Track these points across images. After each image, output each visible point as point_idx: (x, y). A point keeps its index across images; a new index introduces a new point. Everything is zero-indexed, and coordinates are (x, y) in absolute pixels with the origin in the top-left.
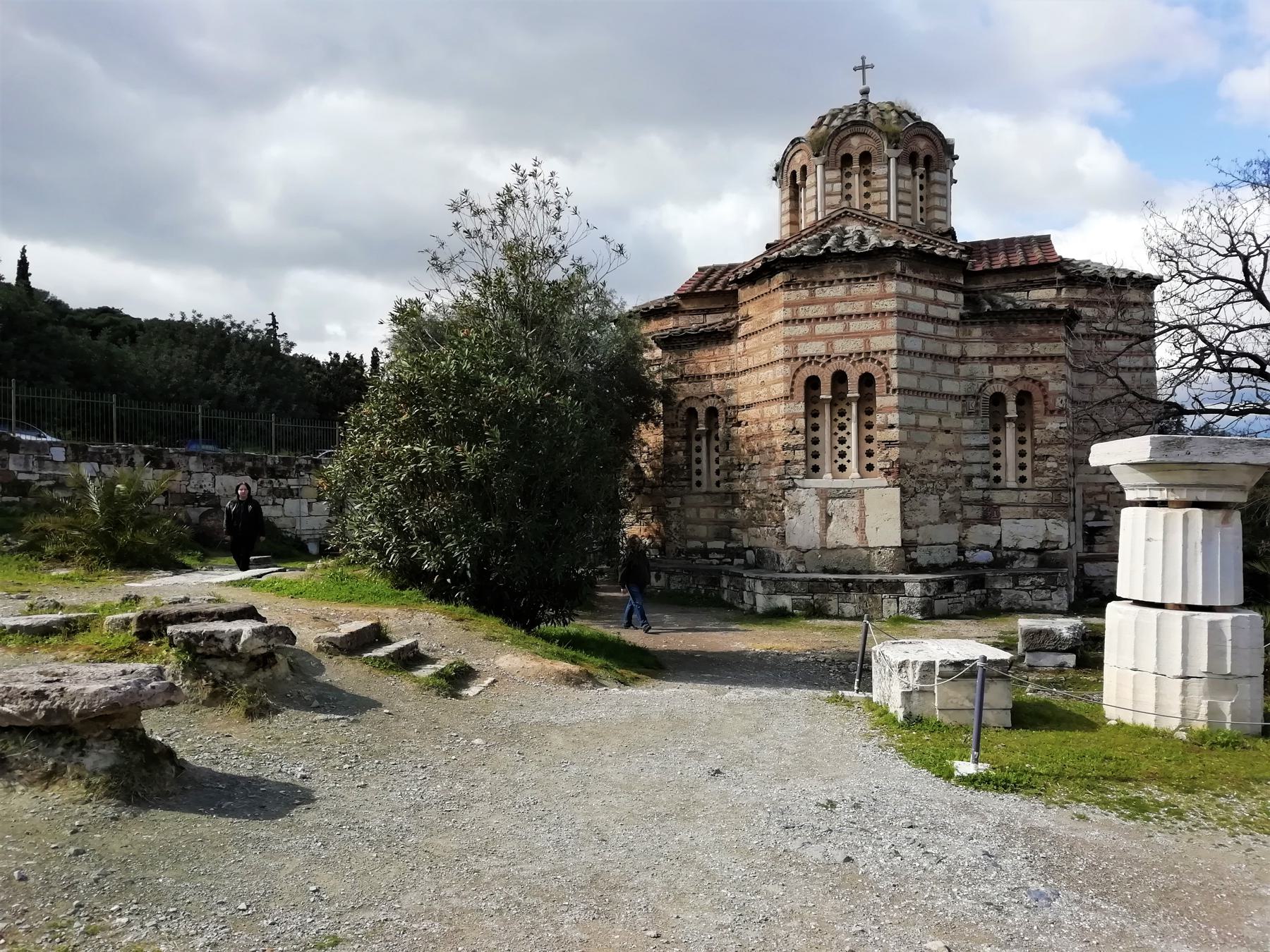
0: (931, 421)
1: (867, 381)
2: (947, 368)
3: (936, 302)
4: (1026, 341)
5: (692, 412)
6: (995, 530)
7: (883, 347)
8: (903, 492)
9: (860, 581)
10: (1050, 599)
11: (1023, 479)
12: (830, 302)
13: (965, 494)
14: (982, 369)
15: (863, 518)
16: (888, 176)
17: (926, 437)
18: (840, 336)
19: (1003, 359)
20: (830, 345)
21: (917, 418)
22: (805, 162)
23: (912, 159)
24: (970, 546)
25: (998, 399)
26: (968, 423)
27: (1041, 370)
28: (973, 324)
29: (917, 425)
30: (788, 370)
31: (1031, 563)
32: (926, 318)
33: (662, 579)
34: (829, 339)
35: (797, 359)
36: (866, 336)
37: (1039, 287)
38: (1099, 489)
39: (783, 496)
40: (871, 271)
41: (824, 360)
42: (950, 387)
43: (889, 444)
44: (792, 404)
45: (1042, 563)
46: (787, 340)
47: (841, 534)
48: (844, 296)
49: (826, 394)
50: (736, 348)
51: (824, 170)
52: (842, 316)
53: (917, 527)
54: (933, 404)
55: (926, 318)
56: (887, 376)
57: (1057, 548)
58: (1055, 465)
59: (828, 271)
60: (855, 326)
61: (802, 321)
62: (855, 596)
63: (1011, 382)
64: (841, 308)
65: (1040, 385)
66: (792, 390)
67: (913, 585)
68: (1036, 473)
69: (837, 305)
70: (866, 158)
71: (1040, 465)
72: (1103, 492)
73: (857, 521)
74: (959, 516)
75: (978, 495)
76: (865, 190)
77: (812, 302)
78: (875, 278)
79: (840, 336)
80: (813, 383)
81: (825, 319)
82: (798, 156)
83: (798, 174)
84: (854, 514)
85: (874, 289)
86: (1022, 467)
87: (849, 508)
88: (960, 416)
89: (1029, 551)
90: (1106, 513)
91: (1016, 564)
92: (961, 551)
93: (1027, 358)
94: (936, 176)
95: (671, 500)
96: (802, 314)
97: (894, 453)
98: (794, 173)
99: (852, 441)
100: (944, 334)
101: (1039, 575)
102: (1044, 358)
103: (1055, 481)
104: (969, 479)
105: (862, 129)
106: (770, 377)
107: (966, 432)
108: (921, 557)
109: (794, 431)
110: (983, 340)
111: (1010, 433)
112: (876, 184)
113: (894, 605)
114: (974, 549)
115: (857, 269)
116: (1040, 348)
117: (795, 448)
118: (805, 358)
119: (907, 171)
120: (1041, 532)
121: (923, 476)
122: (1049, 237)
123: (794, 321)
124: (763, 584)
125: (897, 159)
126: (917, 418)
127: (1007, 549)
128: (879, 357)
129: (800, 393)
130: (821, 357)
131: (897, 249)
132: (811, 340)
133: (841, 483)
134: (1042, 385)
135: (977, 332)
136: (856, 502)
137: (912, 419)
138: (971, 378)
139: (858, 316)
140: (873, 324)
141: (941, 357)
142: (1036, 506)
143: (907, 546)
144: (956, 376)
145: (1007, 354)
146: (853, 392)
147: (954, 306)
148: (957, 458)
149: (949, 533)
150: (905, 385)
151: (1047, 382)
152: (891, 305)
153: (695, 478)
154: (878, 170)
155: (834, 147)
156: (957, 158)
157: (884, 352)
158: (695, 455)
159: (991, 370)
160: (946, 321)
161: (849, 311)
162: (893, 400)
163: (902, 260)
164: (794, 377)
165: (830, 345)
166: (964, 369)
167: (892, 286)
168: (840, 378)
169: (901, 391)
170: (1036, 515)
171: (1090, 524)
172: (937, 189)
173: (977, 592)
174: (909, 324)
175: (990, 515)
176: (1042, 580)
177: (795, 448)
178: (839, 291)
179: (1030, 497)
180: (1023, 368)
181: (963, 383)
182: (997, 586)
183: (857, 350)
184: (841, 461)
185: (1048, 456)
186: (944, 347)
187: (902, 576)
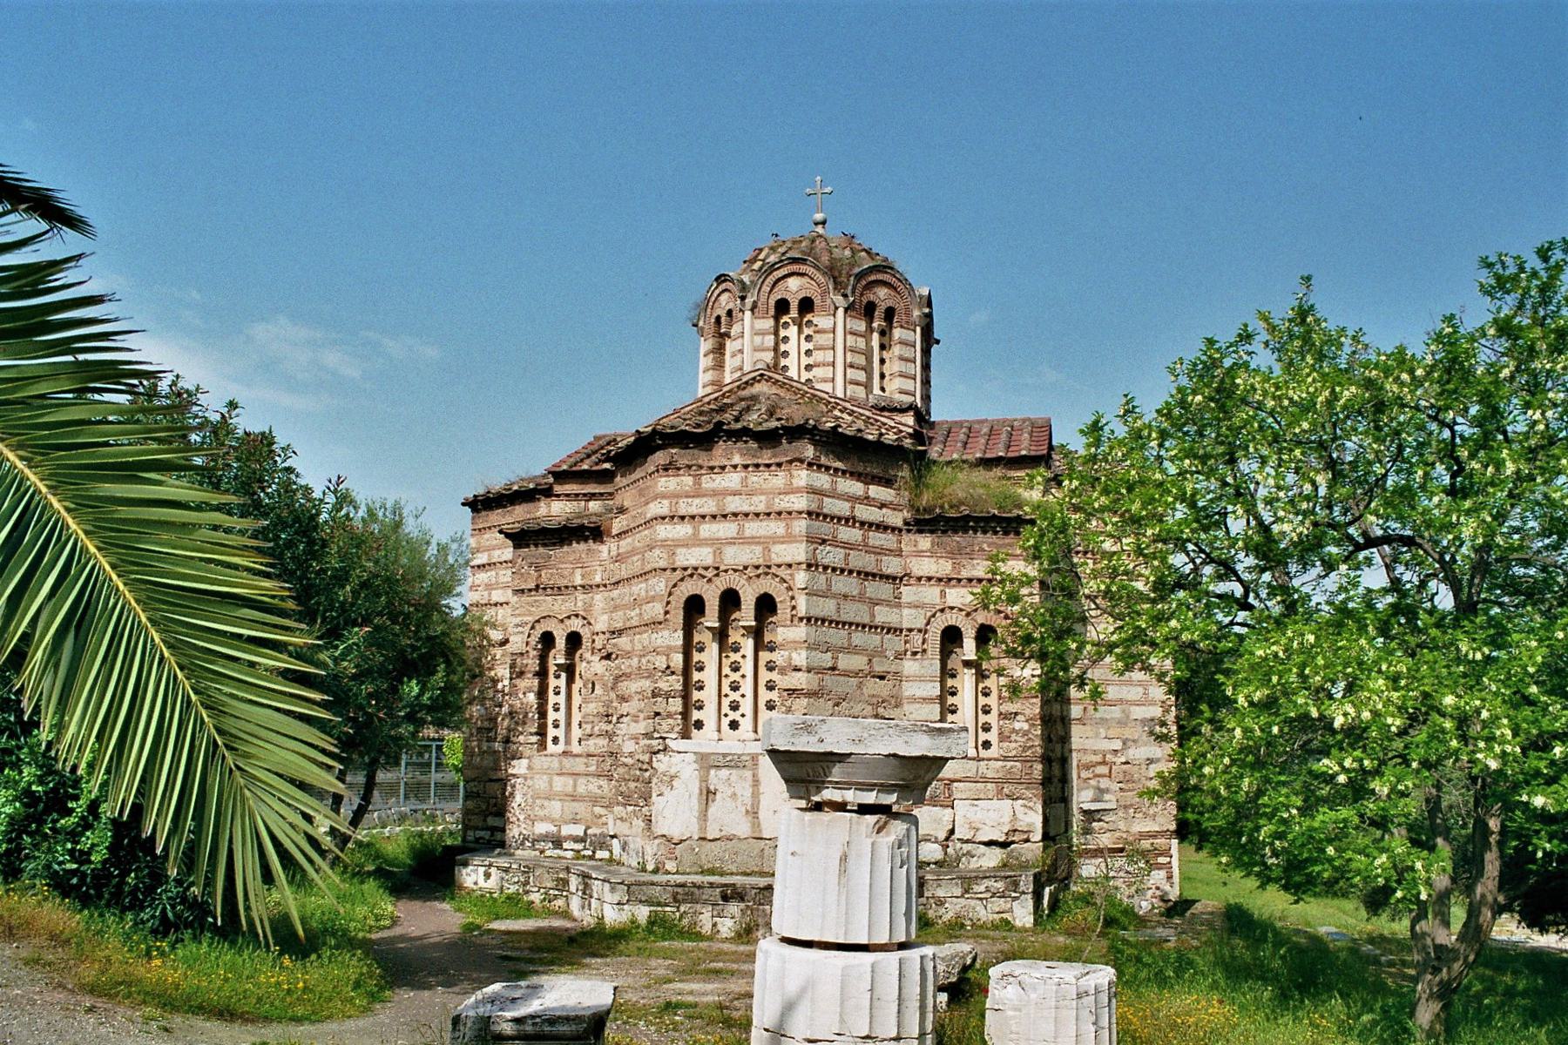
0: (858, 662)
1: (766, 605)
5: (548, 640)
7: (788, 560)
10: (1011, 910)
11: (987, 745)
14: (931, 594)
15: (756, 795)
18: (731, 542)
19: (959, 580)
20: (718, 553)
21: (835, 658)
22: (731, 306)
23: (869, 311)
26: (910, 666)
30: (662, 585)
32: (850, 521)
33: (493, 878)
34: (718, 544)
35: (674, 570)
36: (766, 543)
38: (1099, 758)
39: (650, 763)
40: (774, 456)
41: (709, 574)
44: (666, 633)
48: (739, 487)
50: (606, 550)
52: (735, 515)
54: (858, 638)
55: (850, 521)
56: (793, 598)
57: (1027, 841)
58: (1026, 726)
60: (753, 528)
61: (683, 518)
62: (734, 908)
64: (733, 504)
66: (667, 613)
68: (1003, 737)
69: (730, 498)
70: (806, 305)
72: (1104, 763)
73: (749, 801)
76: (805, 346)
77: (698, 493)
78: (779, 465)
79: (731, 542)
80: (694, 606)
81: (714, 517)
82: (725, 296)
84: (746, 792)
85: (778, 480)
86: (987, 728)
90: (1107, 791)
95: (514, 762)
98: (718, 318)
100: (877, 543)
103: (1025, 749)
105: (803, 268)
106: (643, 593)
110: (932, 554)
117: (668, 696)
118: (685, 569)
119: (861, 326)
120: (1007, 818)
123: (672, 517)
124: (613, 890)
126: (835, 658)
128: (783, 572)
129: (678, 617)
130: (706, 569)
132: (694, 545)
135: (925, 541)
136: (748, 774)
137: (826, 659)
139: (757, 515)
140: (776, 527)
141: (874, 575)
145: (965, 574)
150: (817, 612)
155: (766, 288)
157: (790, 566)
158: (552, 699)
159: (943, 594)
160: (882, 527)
161: (746, 509)
162: (800, 632)
163: (815, 443)
165: (718, 553)
166: (908, 593)
167: (802, 477)
170: (1000, 795)
171: (1086, 807)
174: (825, 528)
176: (1000, 885)
177: (668, 696)
178: (732, 480)
182: (940, 893)
184: (733, 715)
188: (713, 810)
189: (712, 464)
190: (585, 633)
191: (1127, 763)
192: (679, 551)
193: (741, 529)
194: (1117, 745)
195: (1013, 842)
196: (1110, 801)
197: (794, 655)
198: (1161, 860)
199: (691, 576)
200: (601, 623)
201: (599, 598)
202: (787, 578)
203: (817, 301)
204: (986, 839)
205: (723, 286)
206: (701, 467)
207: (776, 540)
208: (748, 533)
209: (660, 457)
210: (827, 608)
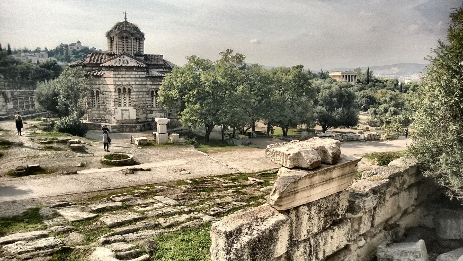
0: (141, 96)
1: (129, 89)
2: (143, 86)
14: (149, 86)
17: (140, 99)
23: (136, 39)
25: (152, 92)
26: (147, 96)
32: (139, 78)
36: (129, 81)
37: (160, 68)
42: (144, 90)
43: (134, 101)
46: (114, 81)
47: (126, 117)
49: (122, 92)
54: (141, 93)
55: (139, 78)
60: (127, 79)
63: (155, 89)
64: (124, 76)
67: (138, 126)
70: (127, 38)
75: (149, 109)
77: (119, 74)
85: (130, 73)
87: (127, 112)
88: (146, 95)
92: (146, 119)
94: (141, 42)
96: (117, 76)
97: (134, 103)
98: (111, 37)
99: (127, 100)
104: (148, 106)
108: (139, 121)
109: (116, 98)
110: (150, 81)
111: (155, 97)
115: (127, 69)
117: (116, 101)
119: (135, 41)
131: (134, 66)
133: (125, 108)
135: (149, 80)
137: (137, 96)
138: (147, 88)
140: (130, 79)
143: (137, 119)
144: (145, 88)
146: (127, 92)
147: (145, 75)
149: (144, 116)
152: (134, 76)
153: (94, 105)
154: (129, 41)
160: (143, 78)
162: (134, 93)
167: (134, 73)
168: (124, 88)
169: (136, 92)
170: (159, 112)
172: (141, 45)
174: (136, 79)
175: (151, 112)
178: (124, 73)
187: (136, 125)
188: (124, 116)
190: (99, 91)
196: (172, 112)
200: (102, 90)
201: (101, 86)
207: (130, 81)
209: (113, 69)
210: (137, 90)
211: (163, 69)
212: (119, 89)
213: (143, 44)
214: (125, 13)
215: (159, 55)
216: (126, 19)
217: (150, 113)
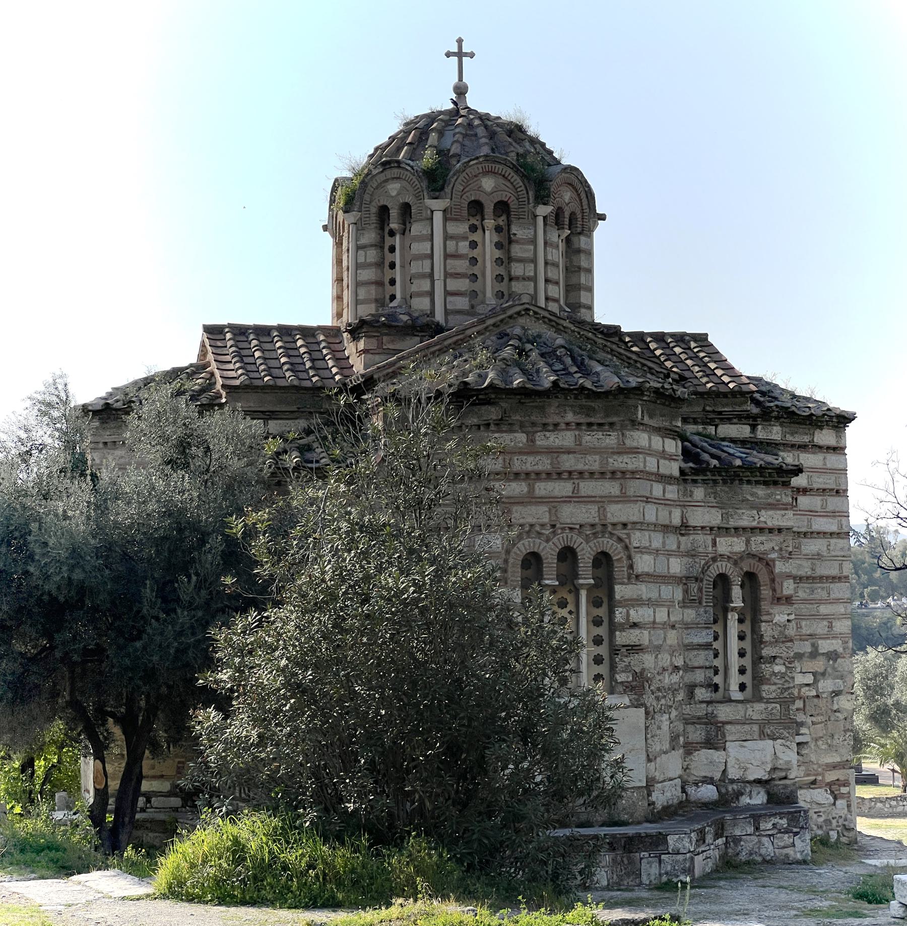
0: (661, 615)
1: (603, 560)
2: (672, 542)
3: (664, 455)
4: (752, 508)
6: (717, 756)
7: (624, 519)
8: (647, 713)
9: (613, 836)
10: (793, 845)
12: (552, 452)
13: (687, 710)
14: (703, 540)
16: (534, 241)
18: (567, 500)
22: (409, 199)
24: (691, 779)
25: (723, 581)
26: (690, 614)
27: (767, 546)
28: (695, 481)
29: (654, 622)
31: (759, 798)
34: (553, 502)
36: (602, 502)
37: (729, 420)
40: (607, 416)
42: (676, 566)
45: (773, 799)
51: (446, 220)
52: (570, 473)
53: (655, 758)
56: (630, 557)
57: (785, 778)
58: (783, 669)
59: (552, 410)
60: (588, 487)
61: (517, 475)
64: (568, 462)
65: (767, 564)
69: (565, 457)
70: (502, 207)
71: (766, 668)
74: (681, 739)
77: (531, 450)
79: (567, 500)
83: (394, 213)
85: (611, 440)
89: (758, 782)
90: (802, 724)
91: (745, 800)
92: (684, 790)
93: (753, 529)
98: (384, 211)
101: (781, 815)
102: (771, 531)
104: (691, 689)
105: (499, 167)
107: (687, 626)
110: (705, 504)
111: (733, 628)
112: (517, 250)
113: (655, 865)
114: (696, 784)
115: (589, 411)
116: (772, 518)
119: (554, 236)
120: (769, 758)
121: (659, 689)
122: (707, 335)
125: (545, 218)
127: (732, 781)
129: (516, 573)
130: (543, 525)
131: (639, 390)
132: (530, 503)
134: (769, 565)
135: (699, 493)
138: (692, 554)
139: (592, 474)
140: (611, 488)
142: (763, 725)
144: (678, 553)
145: (732, 523)
148: (679, 662)
149: (673, 764)
151: (773, 560)
156: (602, 217)
157: (625, 525)
161: (580, 467)
164: (508, 552)
168: (568, 555)
170: (763, 735)
173: (720, 841)
176: (784, 822)
178: (566, 439)
179: (757, 711)
180: (748, 542)
181: (685, 560)
182: (737, 832)
183: (591, 521)
185: (775, 657)
186: (670, 513)
189: (545, 421)
191: (818, 696)
192: (515, 508)
193: (576, 489)
194: (809, 679)
195: (773, 779)
197: (632, 612)
198: (844, 790)
199: (528, 532)
202: (625, 536)
203: (513, 205)
204: (751, 778)
205: (396, 172)
206: (534, 424)
208: (583, 493)
209: (493, 413)
211: (752, 421)
212: (533, 561)
213: (589, 254)
214: (460, 55)
215: (681, 338)
216: (461, 91)
217: (710, 744)
